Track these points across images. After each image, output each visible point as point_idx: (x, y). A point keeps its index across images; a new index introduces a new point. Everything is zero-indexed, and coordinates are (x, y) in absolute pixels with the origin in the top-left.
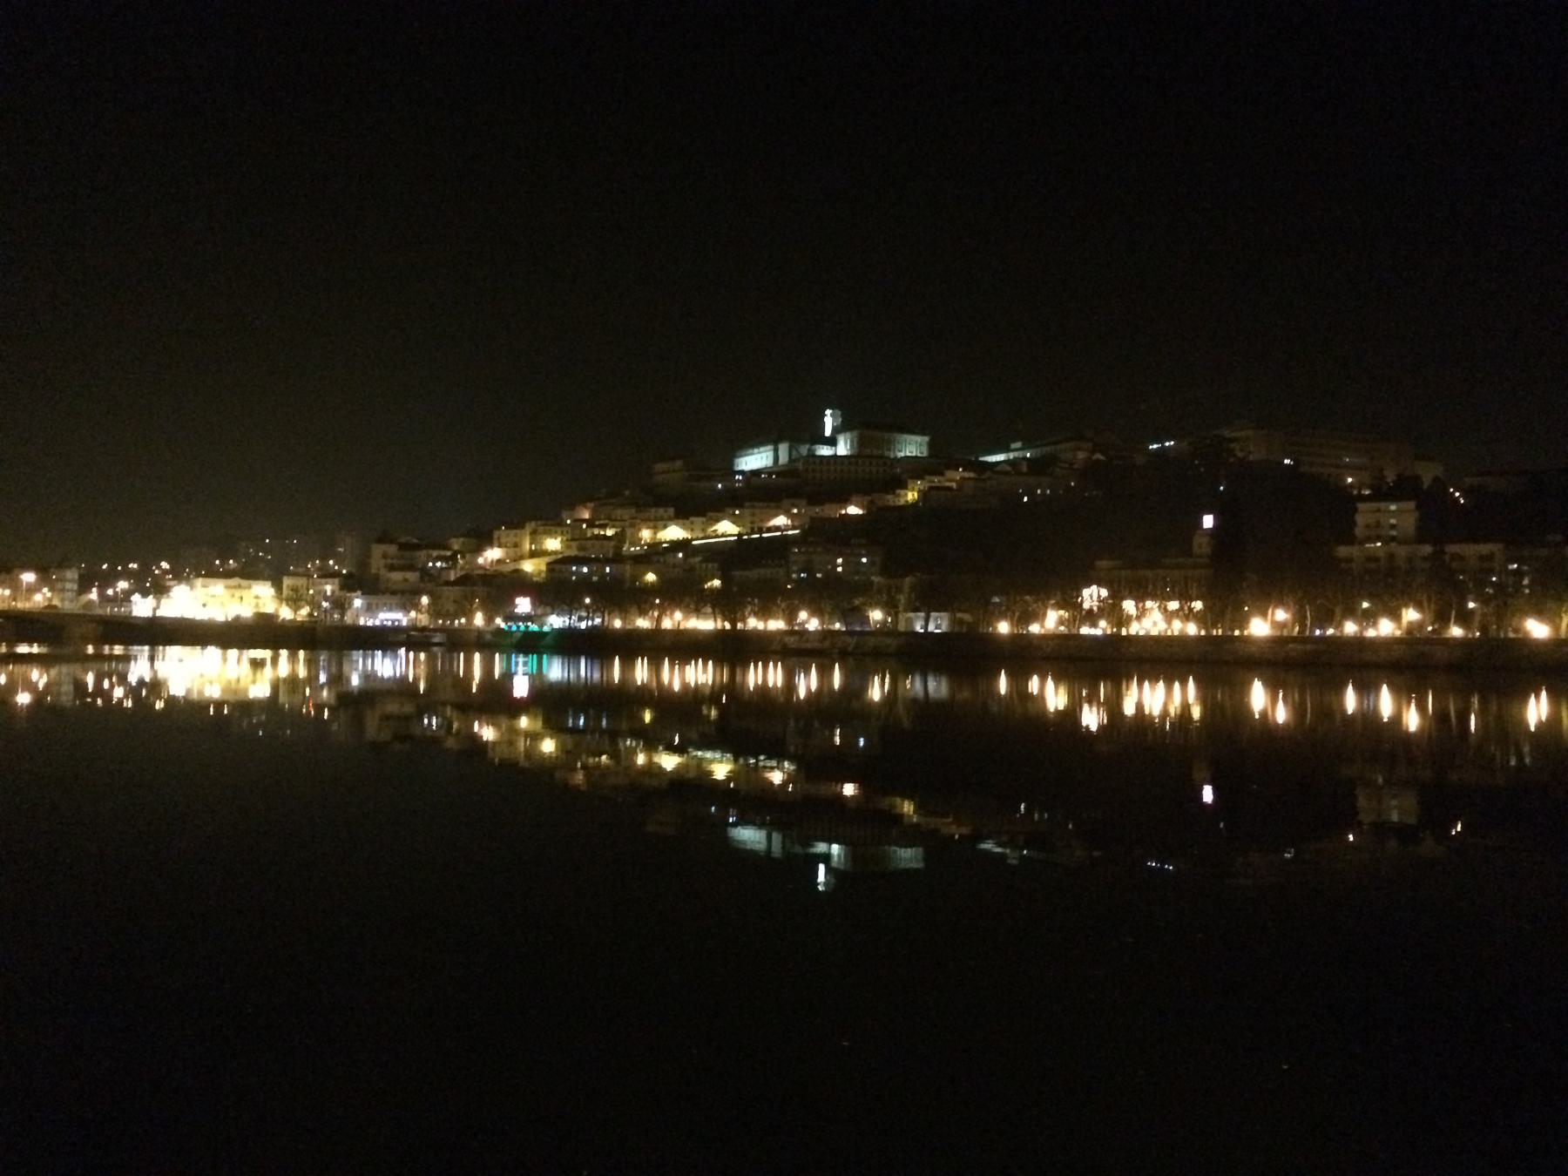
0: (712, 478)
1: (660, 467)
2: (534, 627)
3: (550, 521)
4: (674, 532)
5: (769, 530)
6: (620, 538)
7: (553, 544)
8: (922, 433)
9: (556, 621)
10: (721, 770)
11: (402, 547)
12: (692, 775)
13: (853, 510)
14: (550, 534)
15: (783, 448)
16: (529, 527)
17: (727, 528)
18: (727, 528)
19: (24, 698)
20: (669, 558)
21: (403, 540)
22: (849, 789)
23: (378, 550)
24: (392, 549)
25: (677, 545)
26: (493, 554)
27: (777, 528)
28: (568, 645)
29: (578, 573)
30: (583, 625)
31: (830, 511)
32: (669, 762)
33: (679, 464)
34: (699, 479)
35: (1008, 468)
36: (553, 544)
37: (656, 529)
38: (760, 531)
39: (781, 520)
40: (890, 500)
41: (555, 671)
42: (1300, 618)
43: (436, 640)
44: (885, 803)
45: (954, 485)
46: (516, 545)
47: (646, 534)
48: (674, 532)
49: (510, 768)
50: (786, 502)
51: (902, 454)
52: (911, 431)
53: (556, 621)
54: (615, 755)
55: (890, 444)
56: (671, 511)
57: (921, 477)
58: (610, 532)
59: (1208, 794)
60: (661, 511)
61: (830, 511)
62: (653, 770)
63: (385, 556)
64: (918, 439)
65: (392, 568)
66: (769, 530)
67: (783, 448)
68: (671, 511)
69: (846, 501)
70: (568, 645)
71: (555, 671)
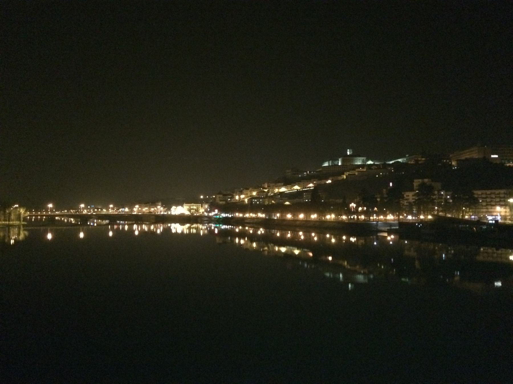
0: (298, 174)
1: (288, 171)
2: (218, 217)
3: (255, 188)
4: (283, 189)
5: (308, 188)
6: (268, 192)
7: (254, 194)
8: (363, 157)
9: (224, 215)
10: (297, 252)
11: (224, 195)
12: (289, 253)
13: (329, 181)
14: (254, 191)
15: (330, 162)
16: (250, 189)
17: (297, 187)
18: (297, 187)
19: (137, 233)
20: (277, 197)
21: (225, 193)
22: (330, 258)
23: (218, 196)
24: (221, 196)
25: (281, 194)
26: (242, 196)
27: (310, 187)
28: (225, 221)
29: (255, 202)
30: (230, 216)
31: (323, 182)
32: (283, 250)
33: (290, 171)
34: (295, 174)
35: (376, 167)
36: (254, 194)
37: (279, 189)
38: (306, 188)
39: (311, 185)
40: (340, 178)
41: (224, 227)
42: (336, 215)
43: (206, 219)
44: (340, 262)
45: (357, 174)
46: (247, 194)
47: (276, 190)
48: (283, 189)
49: (247, 249)
50: (312, 180)
51: (357, 163)
52: (360, 156)
53: (224, 215)
54: (268, 247)
55: (353, 161)
56: (282, 184)
57: (349, 171)
58: (266, 190)
59: (392, 260)
60: (280, 184)
61: (323, 182)
62: (279, 251)
63: (219, 198)
64: (363, 158)
65: (221, 201)
66: (308, 188)
67: (330, 162)
68: (282, 184)
69: (327, 179)
70: (225, 221)
71: (224, 227)
